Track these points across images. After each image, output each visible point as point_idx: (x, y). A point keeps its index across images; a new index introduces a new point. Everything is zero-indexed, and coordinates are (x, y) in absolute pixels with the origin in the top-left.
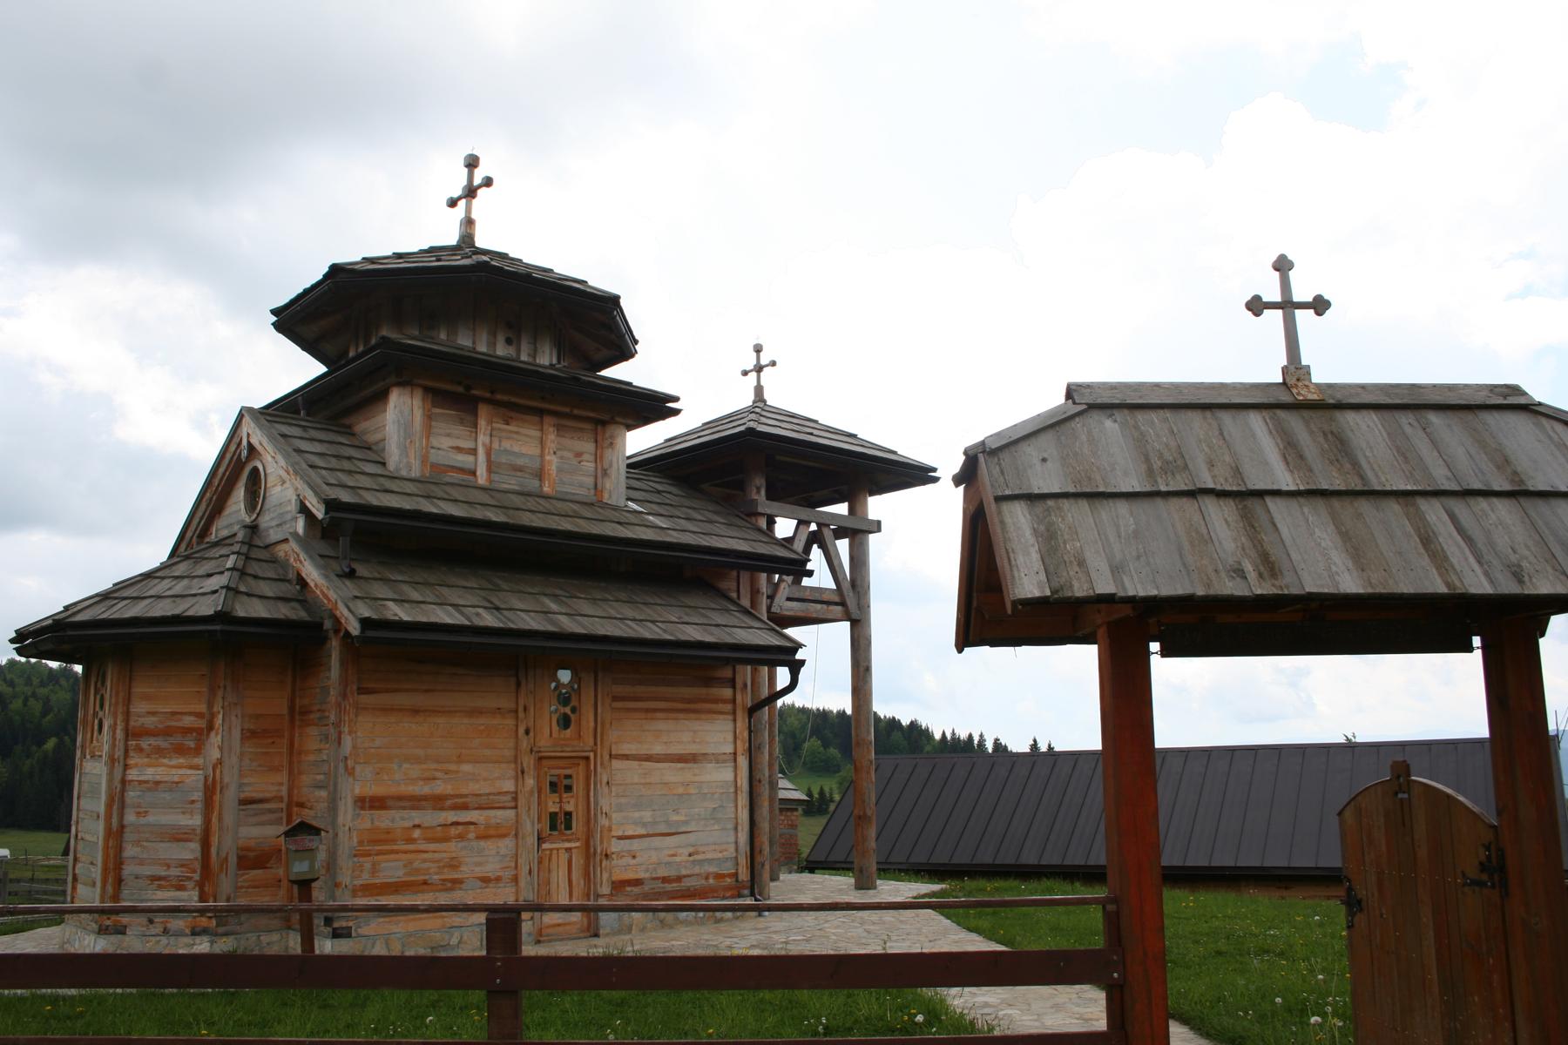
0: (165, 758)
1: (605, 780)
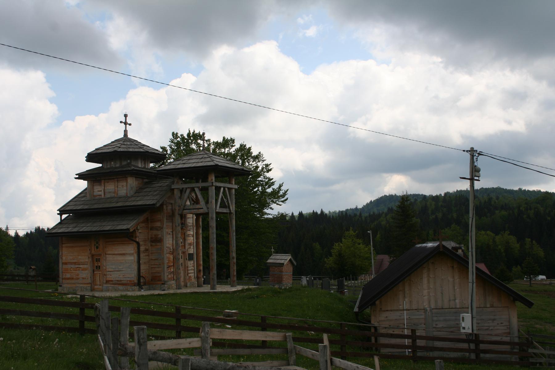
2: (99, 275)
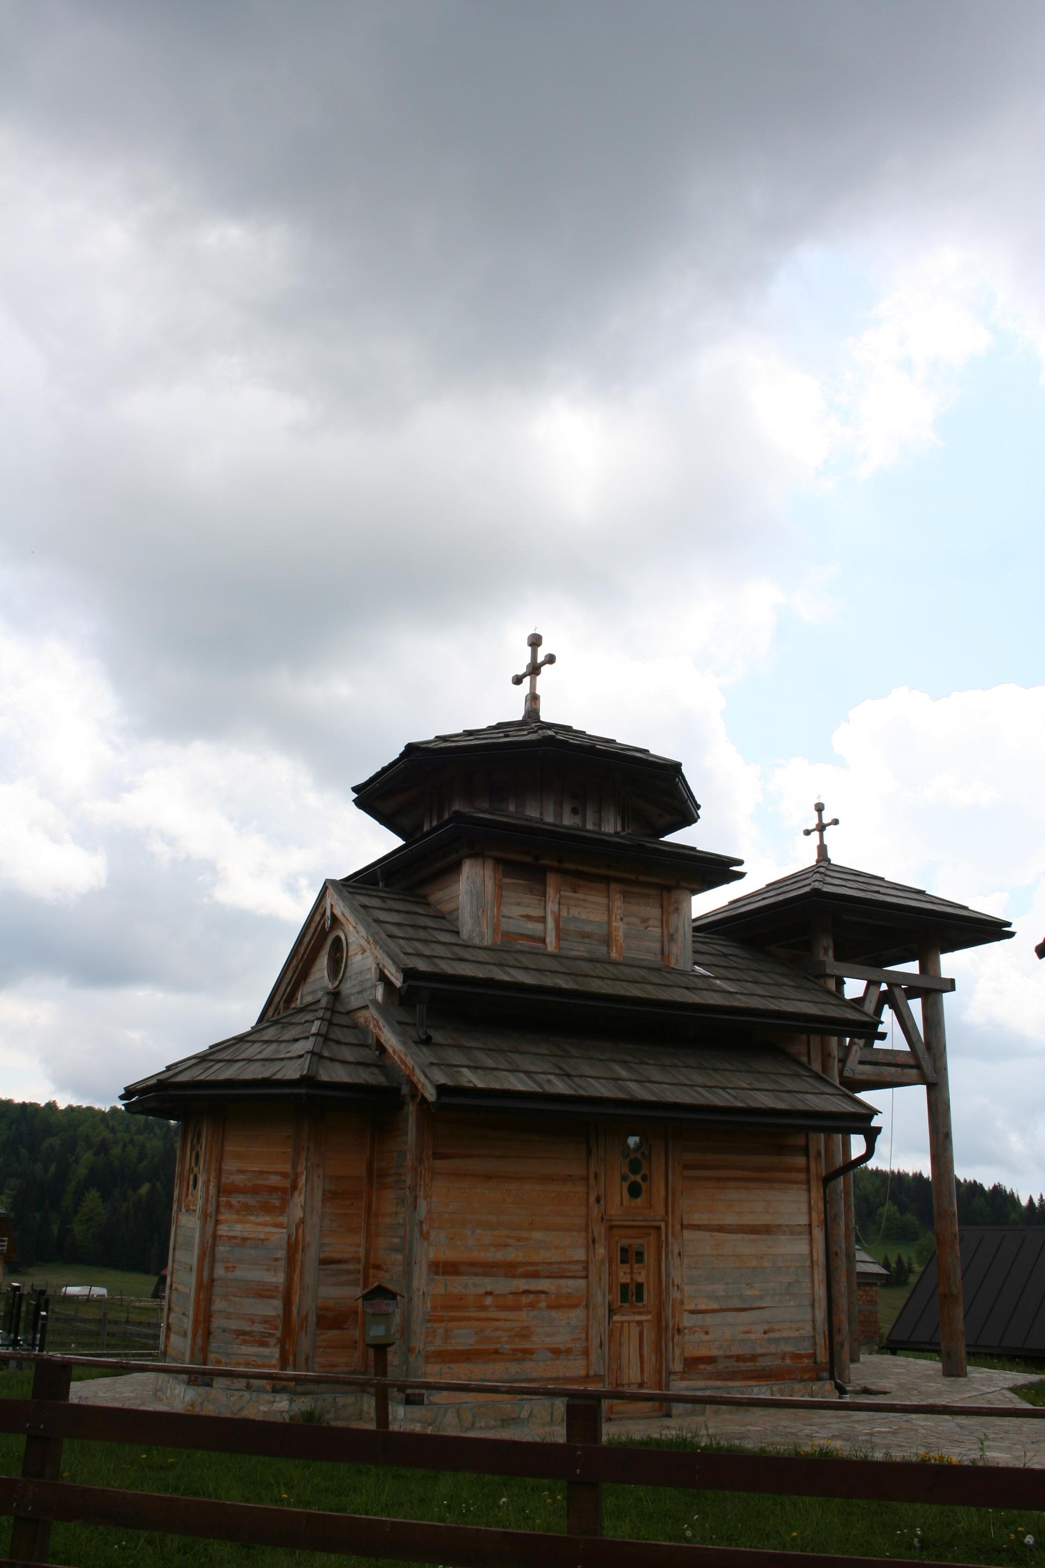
0: (252, 1215)
1: (676, 1251)
2: (638, 1329)
